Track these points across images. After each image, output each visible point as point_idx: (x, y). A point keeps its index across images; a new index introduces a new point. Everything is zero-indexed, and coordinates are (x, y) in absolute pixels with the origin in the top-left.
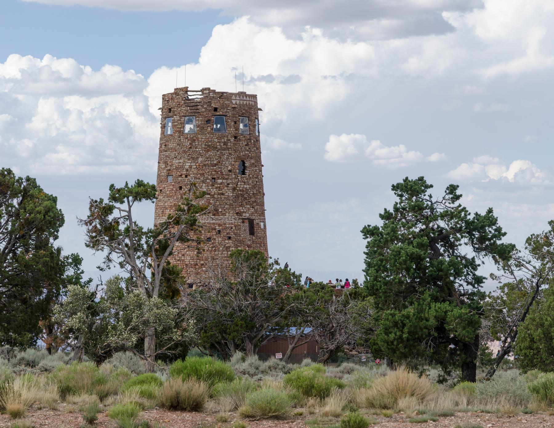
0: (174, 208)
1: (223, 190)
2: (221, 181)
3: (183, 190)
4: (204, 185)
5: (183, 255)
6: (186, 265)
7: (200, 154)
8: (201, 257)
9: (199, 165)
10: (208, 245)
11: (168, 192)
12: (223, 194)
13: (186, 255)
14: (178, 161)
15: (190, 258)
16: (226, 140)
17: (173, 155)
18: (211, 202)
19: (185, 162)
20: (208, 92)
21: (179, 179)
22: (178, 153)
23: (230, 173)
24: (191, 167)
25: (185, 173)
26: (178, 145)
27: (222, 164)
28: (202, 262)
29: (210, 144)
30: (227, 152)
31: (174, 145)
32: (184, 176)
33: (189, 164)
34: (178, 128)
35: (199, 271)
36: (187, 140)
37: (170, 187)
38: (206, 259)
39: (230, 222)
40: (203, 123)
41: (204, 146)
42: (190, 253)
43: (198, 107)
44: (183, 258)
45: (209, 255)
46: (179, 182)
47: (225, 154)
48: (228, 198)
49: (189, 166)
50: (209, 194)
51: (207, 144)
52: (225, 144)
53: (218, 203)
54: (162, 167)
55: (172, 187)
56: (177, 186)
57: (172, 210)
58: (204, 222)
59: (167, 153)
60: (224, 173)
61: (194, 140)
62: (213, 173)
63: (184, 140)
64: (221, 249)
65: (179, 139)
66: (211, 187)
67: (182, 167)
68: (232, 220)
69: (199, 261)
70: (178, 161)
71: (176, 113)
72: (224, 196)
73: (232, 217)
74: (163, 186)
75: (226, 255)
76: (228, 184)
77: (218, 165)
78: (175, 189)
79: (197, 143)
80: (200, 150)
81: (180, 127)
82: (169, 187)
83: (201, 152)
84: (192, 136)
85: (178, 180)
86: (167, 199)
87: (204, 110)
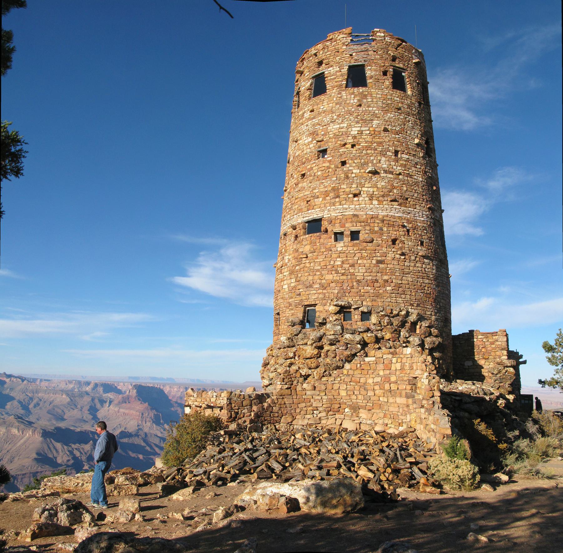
0: (332, 195)
1: (410, 170)
2: (407, 157)
3: (348, 165)
4: (383, 159)
5: (353, 266)
6: (359, 281)
7: (375, 115)
8: (383, 269)
9: (374, 131)
10: (393, 250)
11: (319, 173)
12: (411, 176)
13: (356, 266)
14: (338, 126)
15: (364, 271)
16: (409, 102)
17: (327, 119)
18: (394, 184)
19: (349, 126)
20: (383, 35)
21: (340, 151)
22: (338, 116)
23: (418, 150)
24: (361, 133)
25: (352, 141)
26: (336, 104)
27: (407, 132)
28: (386, 277)
29: (389, 102)
30: (412, 118)
31: (331, 105)
32: (349, 146)
33: (359, 129)
34: (336, 82)
35: (381, 291)
36: (353, 96)
37: (324, 165)
38: (393, 273)
39: (422, 219)
40: (378, 73)
41: (380, 104)
42: (365, 261)
43: (370, 53)
44: (352, 271)
45: (397, 267)
46: (341, 155)
47: (409, 121)
48: (416, 183)
49: (358, 131)
50: (392, 173)
51: (384, 102)
52: (409, 106)
53: (405, 189)
54: (306, 141)
55: (327, 164)
56: (338, 161)
57: (328, 198)
58: (386, 214)
59: (315, 121)
60: (410, 146)
61: (365, 96)
62: (395, 143)
63: (348, 97)
64: (413, 258)
65: (339, 96)
66: (394, 163)
67: (347, 134)
68: (423, 217)
69: (379, 275)
70: (338, 126)
71: (332, 63)
72: (411, 179)
73: (424, 213)
74: (309, 167)
75: (420, 269)
76: (416, 164)
77: (402, 134)
78: (333, 166)
79: (370, 100)
80: (375, 109)
81: (341, 79)
82: (320, 166)
83: (377, 112)
84: (361, 91)
85: (339, 152)
86: (318, 183)
87: (379, 57)
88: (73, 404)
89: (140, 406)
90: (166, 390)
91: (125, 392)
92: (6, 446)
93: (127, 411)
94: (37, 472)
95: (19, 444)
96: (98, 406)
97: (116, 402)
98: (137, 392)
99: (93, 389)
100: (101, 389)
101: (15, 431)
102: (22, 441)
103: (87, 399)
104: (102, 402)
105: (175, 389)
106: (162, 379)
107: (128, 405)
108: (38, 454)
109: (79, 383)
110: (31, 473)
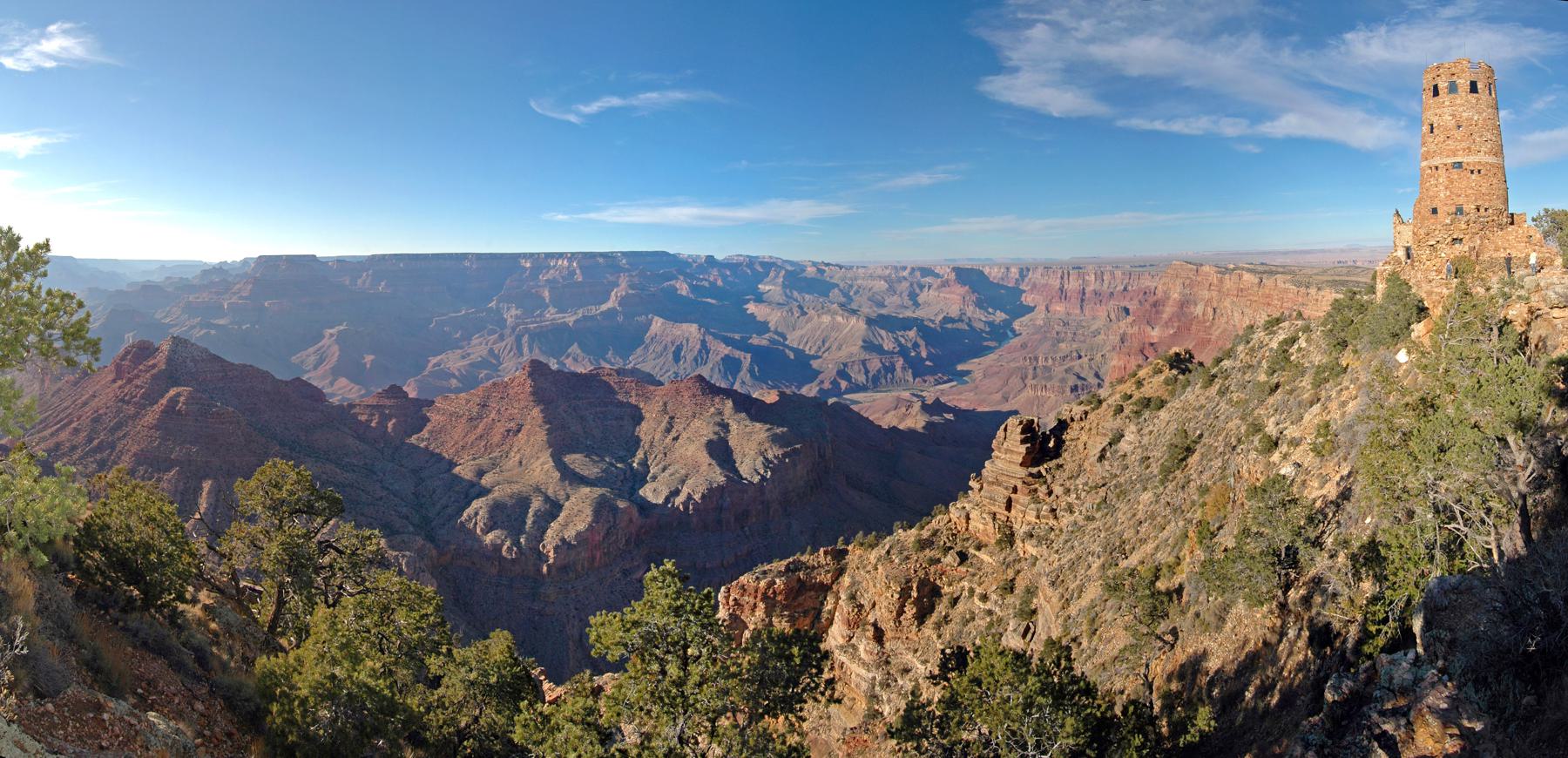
88: (892, 290)
89: (961, 290)
90: (986, 271)
91: (943, 276)
93: (947, 296)
95: (845, 332)
96: (918, 291)
97: (935, 286)
98: (956, 275)
99: (910, 274)
100: (918, 274)
101: (839, 319)
102: (848, 329)
103: (905, 285)
104: (921, 287)
106: (979, 260)
107: (948, 289)
108: (864, 341)
109: (896, 268)
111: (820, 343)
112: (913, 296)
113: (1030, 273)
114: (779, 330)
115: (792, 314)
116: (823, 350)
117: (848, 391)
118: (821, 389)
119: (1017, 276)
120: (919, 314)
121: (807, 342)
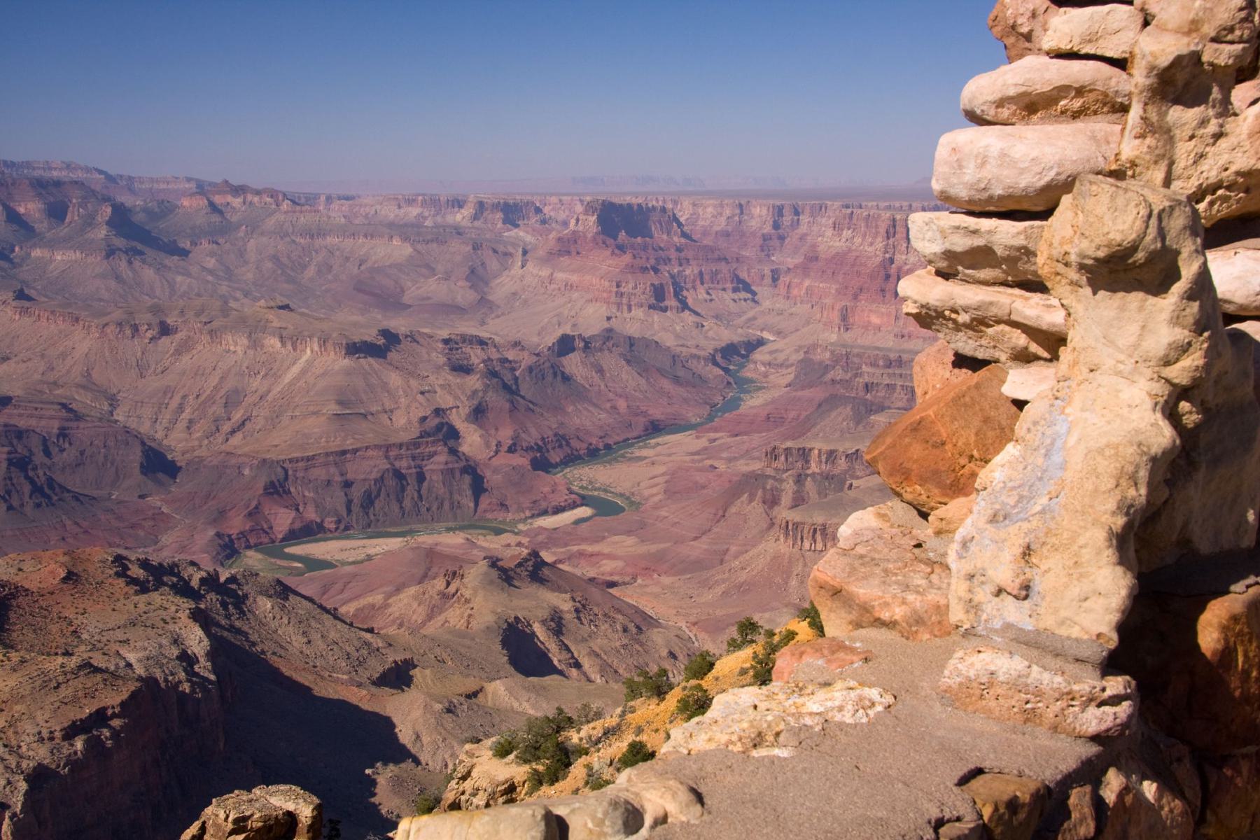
92: (255, 383)
93: (574, 278)
94: (344, 452)
96: (493, 264)
97: (541, 253)
98: (601, 221)
99: (475, 217)
101: (273, 343)
102: (295, 370)
103: (459, 249)
105: (710, 210)
108: (340, 403)
109: (433, 202)
110: (327, 454)
111: (217, 409)
112: (477, 277)
113: (805, 219)
114: (95, 375)
115: (135, 329)
116: (227, 427)
117: (295, 535)
118: (218, 535)
119: (768, 229)
120: (497, 329)
121: (181, 408)
